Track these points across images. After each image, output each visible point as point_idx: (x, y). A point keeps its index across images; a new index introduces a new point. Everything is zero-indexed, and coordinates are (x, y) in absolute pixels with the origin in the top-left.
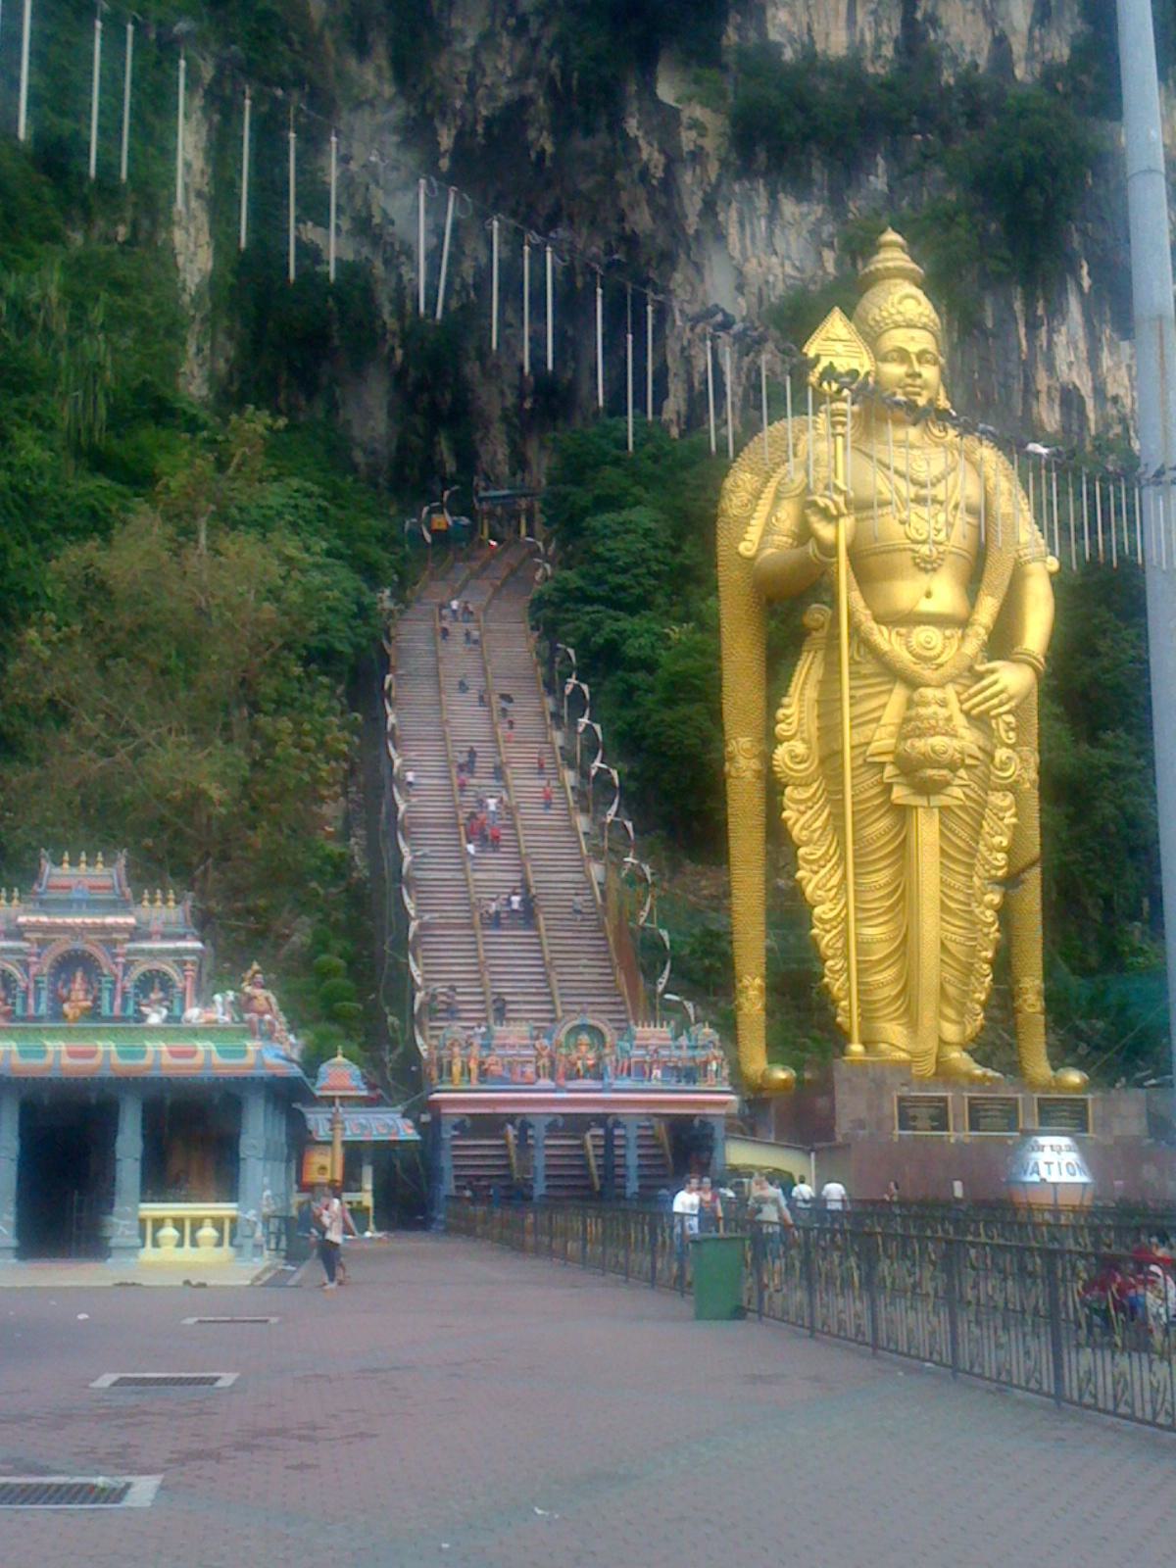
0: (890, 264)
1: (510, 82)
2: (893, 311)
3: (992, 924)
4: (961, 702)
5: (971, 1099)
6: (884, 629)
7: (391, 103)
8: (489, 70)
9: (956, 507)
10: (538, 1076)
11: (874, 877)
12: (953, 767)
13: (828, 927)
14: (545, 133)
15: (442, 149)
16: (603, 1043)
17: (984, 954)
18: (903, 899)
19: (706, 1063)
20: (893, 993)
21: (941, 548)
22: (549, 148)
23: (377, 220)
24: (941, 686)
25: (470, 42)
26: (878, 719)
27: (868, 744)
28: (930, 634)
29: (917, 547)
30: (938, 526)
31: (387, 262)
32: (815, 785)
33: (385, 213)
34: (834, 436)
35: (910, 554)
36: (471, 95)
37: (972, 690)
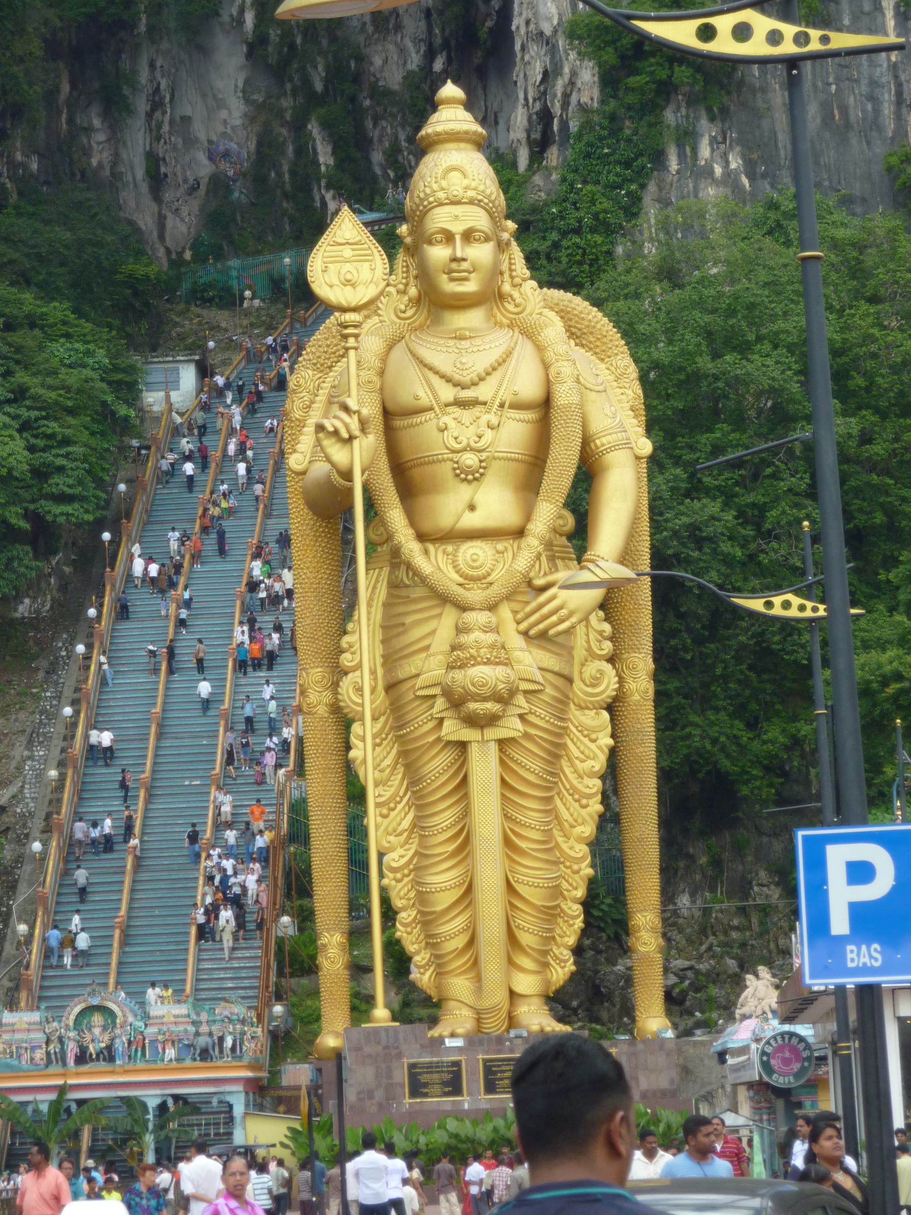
0: (440, 128)
2: (435, 187)
3: (582, 859)
4: (518, 623)
5: (485, 1061)
6: (431, 548)
9: (502, 406)
10: (49, 1062)
11: (436, 820)
12: (504, 698)
13: (399, 876)
16: (114, 1022)
17: (574, 892)
18: (464, 843)
19: (221, 1039)
20: (460, 946)
21: (484, 455)
24: (492, 607)
26: (427, 648)
27: (418, 675)
28: (478, 551)
29: (456, 457)
30: (479, 432)
32: (382, 719)
34: (347, 349)
35: (449, 465)
37: (528, 609)
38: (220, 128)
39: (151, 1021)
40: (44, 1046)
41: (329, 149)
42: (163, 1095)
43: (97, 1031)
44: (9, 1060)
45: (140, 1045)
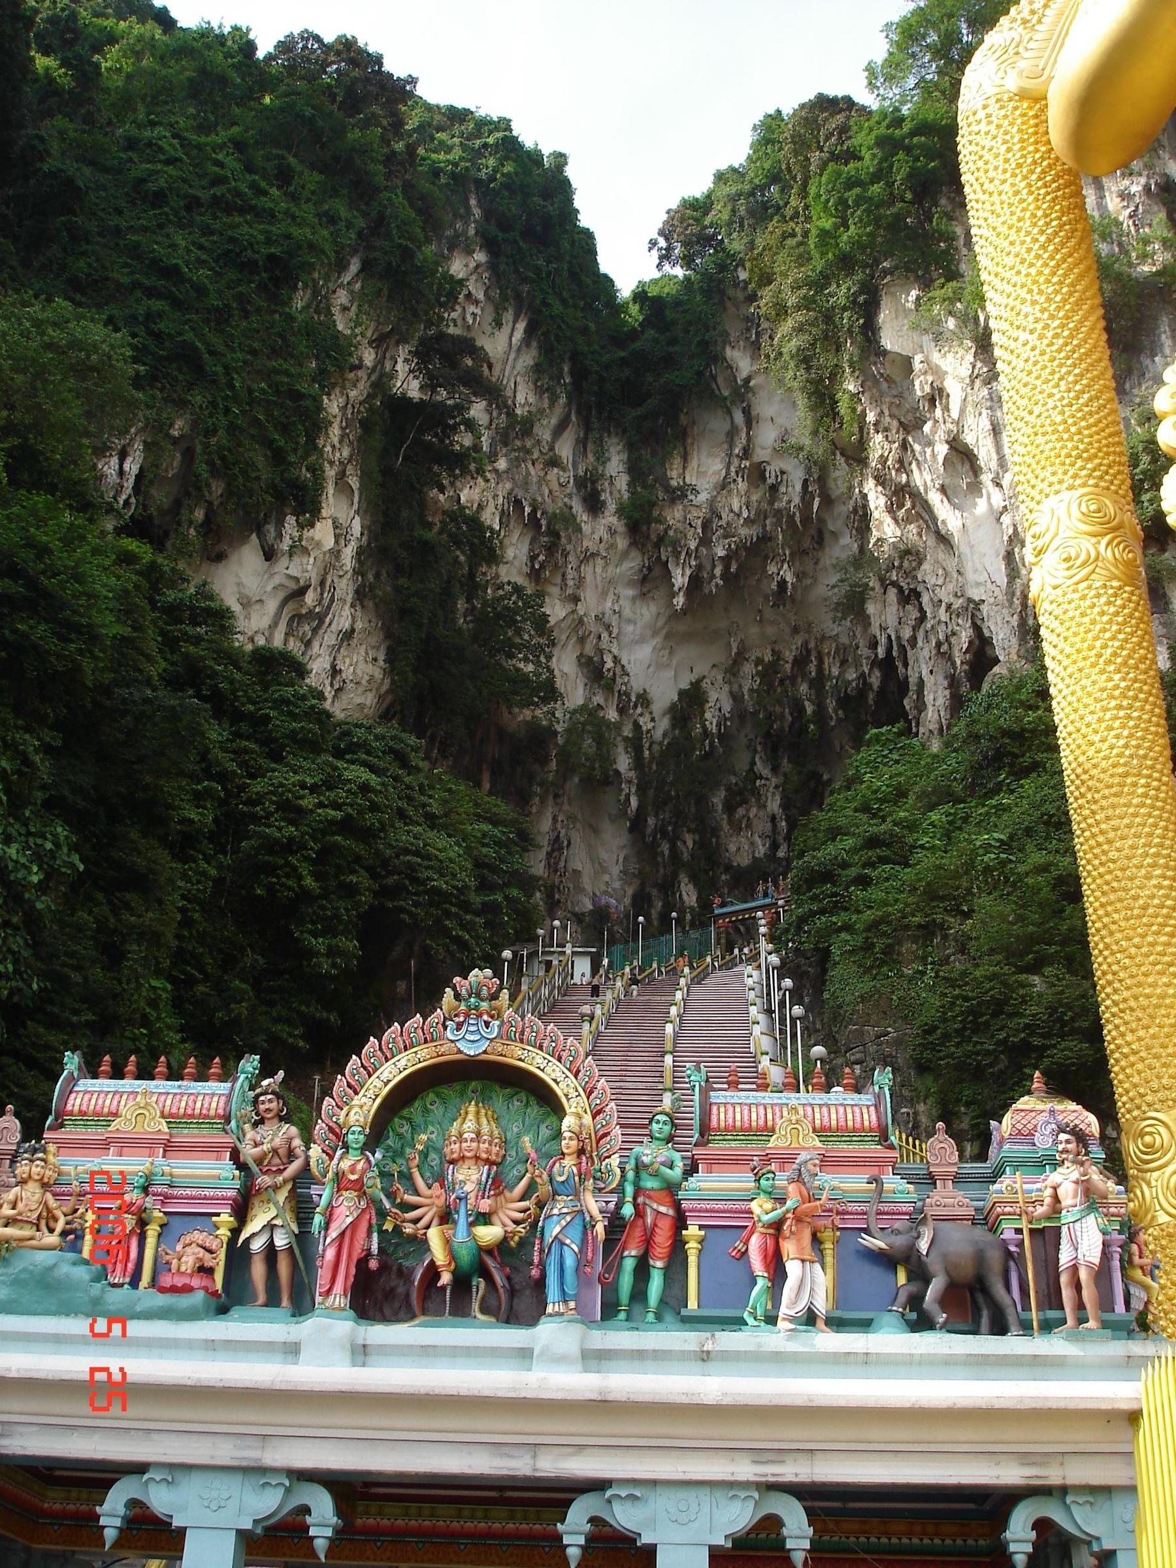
1: (748, 522)
7: (625, 555)
8: (724, 516)
14: (786, 566)
15: (676, 589)
19: (1047, 1238)
22: (790, 578)
23: (609, 664)
25: (703, 497)
31: (621, 711)
33: (616, 660)
36: (705, 541)
38: (603, 888)
39: (717, 1147)
40: (226, 1218)
45: (663, 1239)
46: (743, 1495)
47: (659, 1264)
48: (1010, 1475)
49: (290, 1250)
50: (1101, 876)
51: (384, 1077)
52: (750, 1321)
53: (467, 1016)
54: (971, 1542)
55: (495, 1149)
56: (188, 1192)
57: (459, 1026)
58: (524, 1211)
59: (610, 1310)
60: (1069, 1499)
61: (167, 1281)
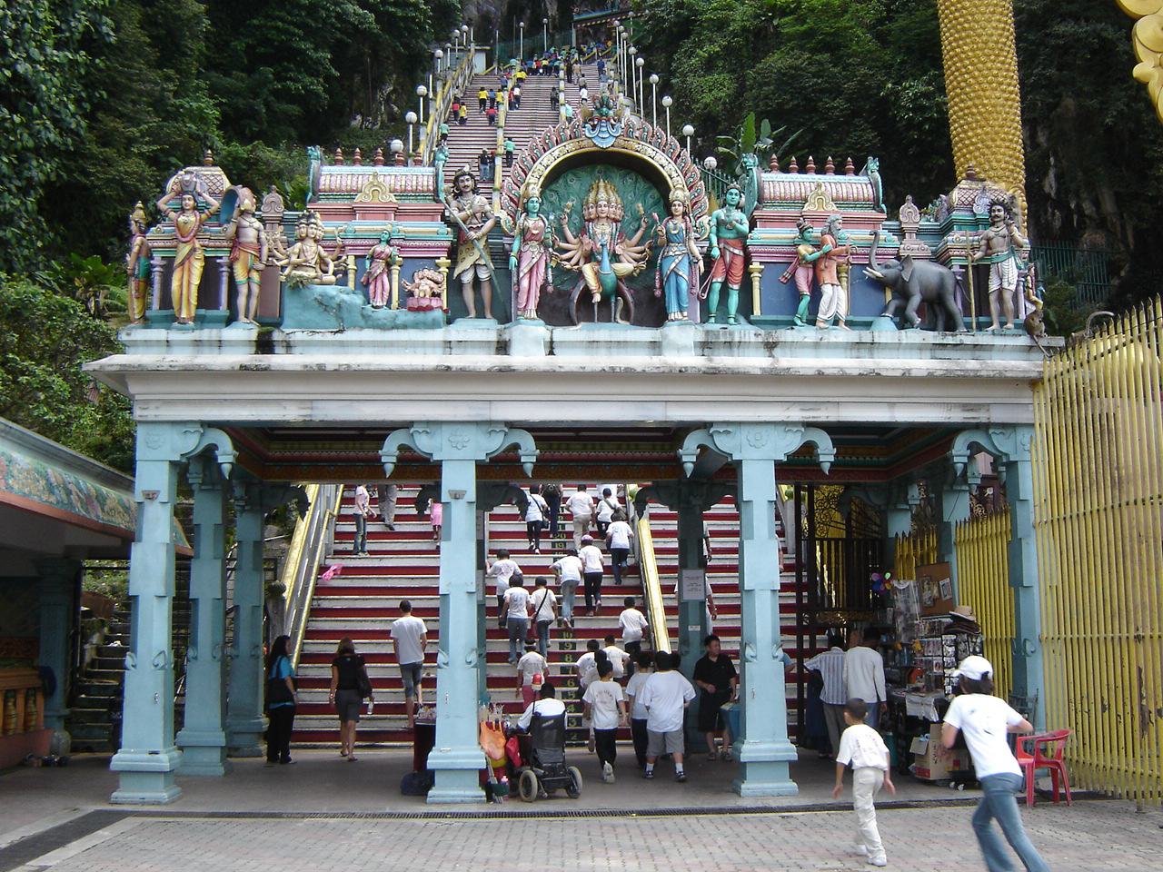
19: (982, 272)
39: (767, 211)
40: (444, 261)
41: (555, 7)
42: (809, 425)
43: (603, 231)
44: (332, 290)
45: (738, 272)
46: (795, 429)
47: (736, 287)
48: (957, 416)
49: (490, 280)
50: (956, 19)
51: (545, 163)
52: (799, 322)
53: (600, 120)
54: (875, 459)
55: (619, 212)
56: (417, 243)
57: (594, 127)
58: (641, 253)
59: (705, 319)
60: (991, 431)
61: (412, 302)
